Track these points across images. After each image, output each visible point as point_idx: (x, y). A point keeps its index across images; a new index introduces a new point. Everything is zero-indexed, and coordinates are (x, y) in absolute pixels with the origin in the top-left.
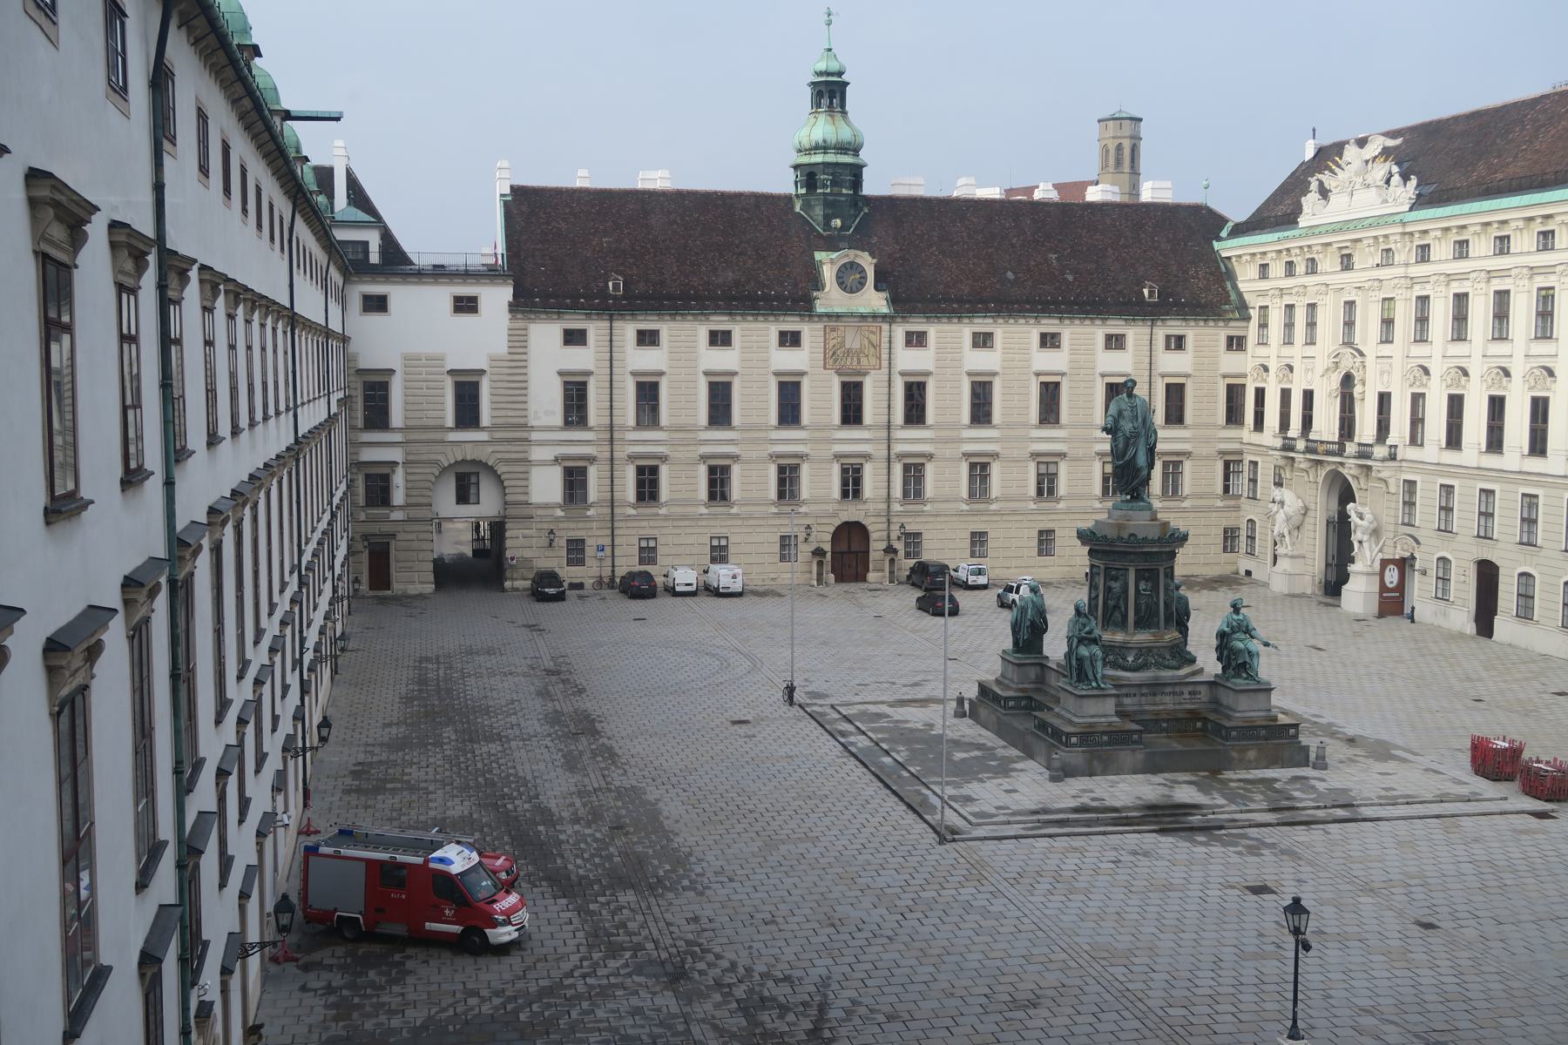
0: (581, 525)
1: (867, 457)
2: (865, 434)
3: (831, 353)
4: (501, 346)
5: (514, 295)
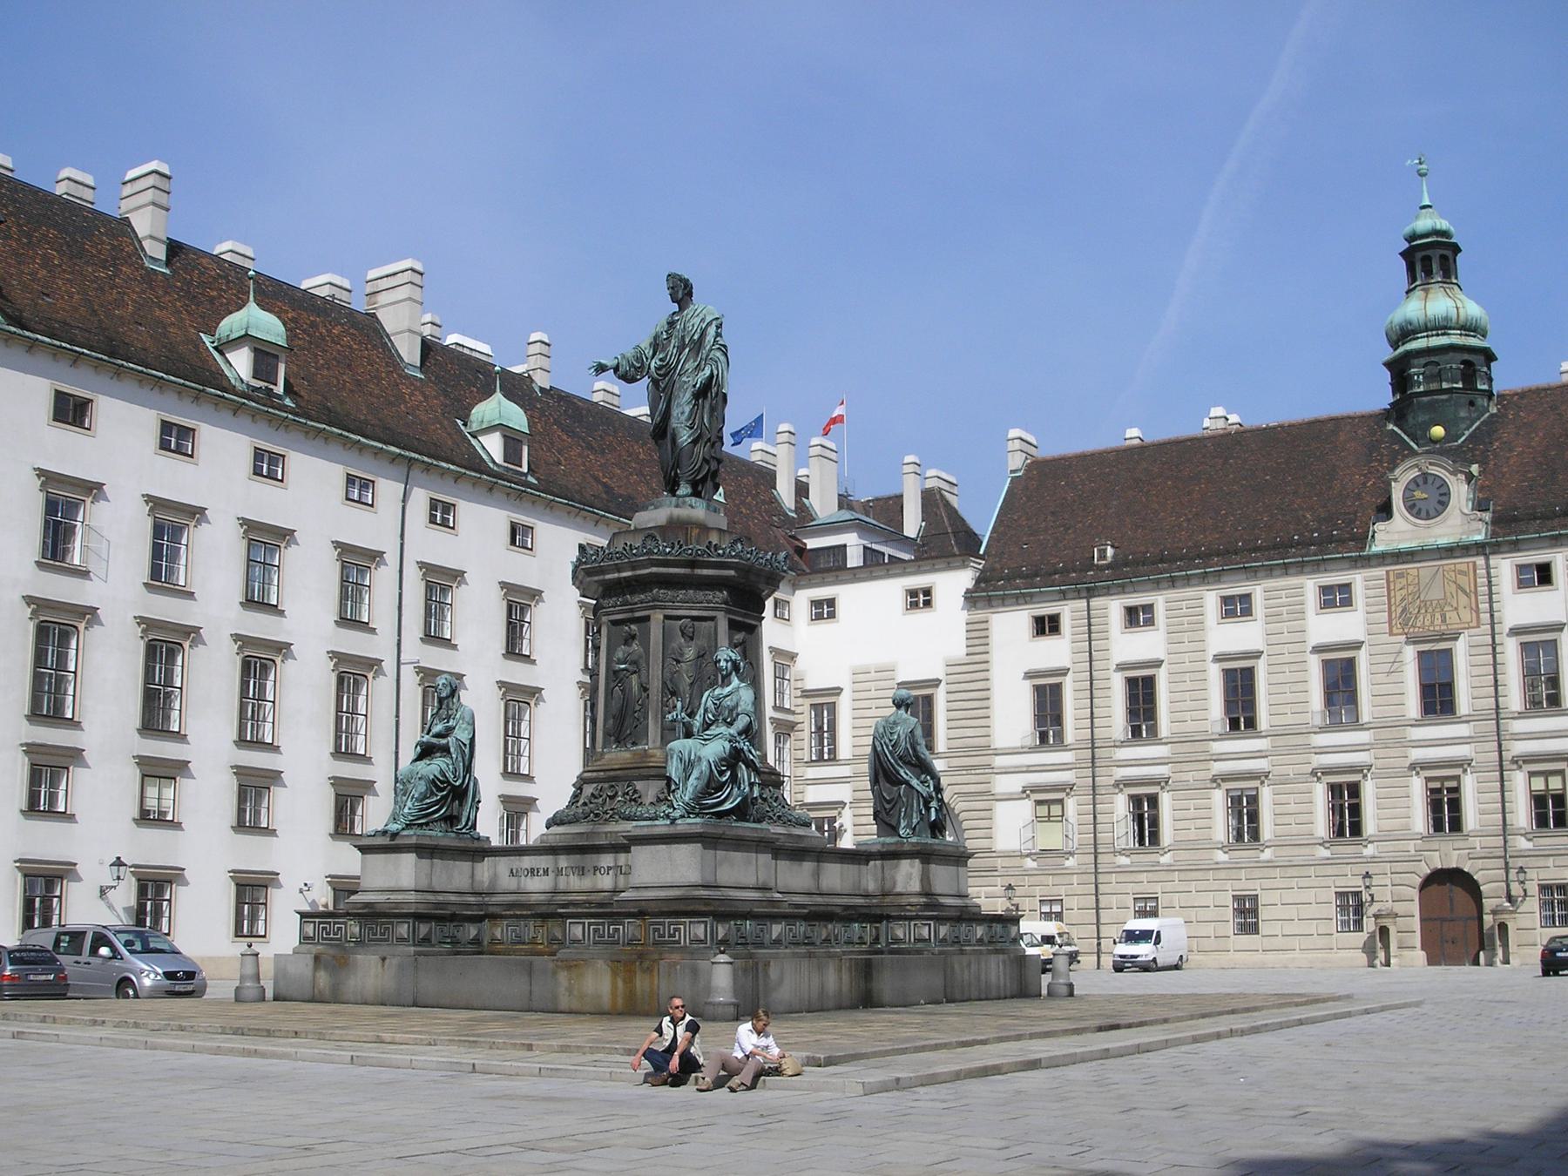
0: (1058, 880)
1: (1463, 764)
2: (1462, 730)
3: (1399, 610)
4: (958, 649)
5: (978, 581)
